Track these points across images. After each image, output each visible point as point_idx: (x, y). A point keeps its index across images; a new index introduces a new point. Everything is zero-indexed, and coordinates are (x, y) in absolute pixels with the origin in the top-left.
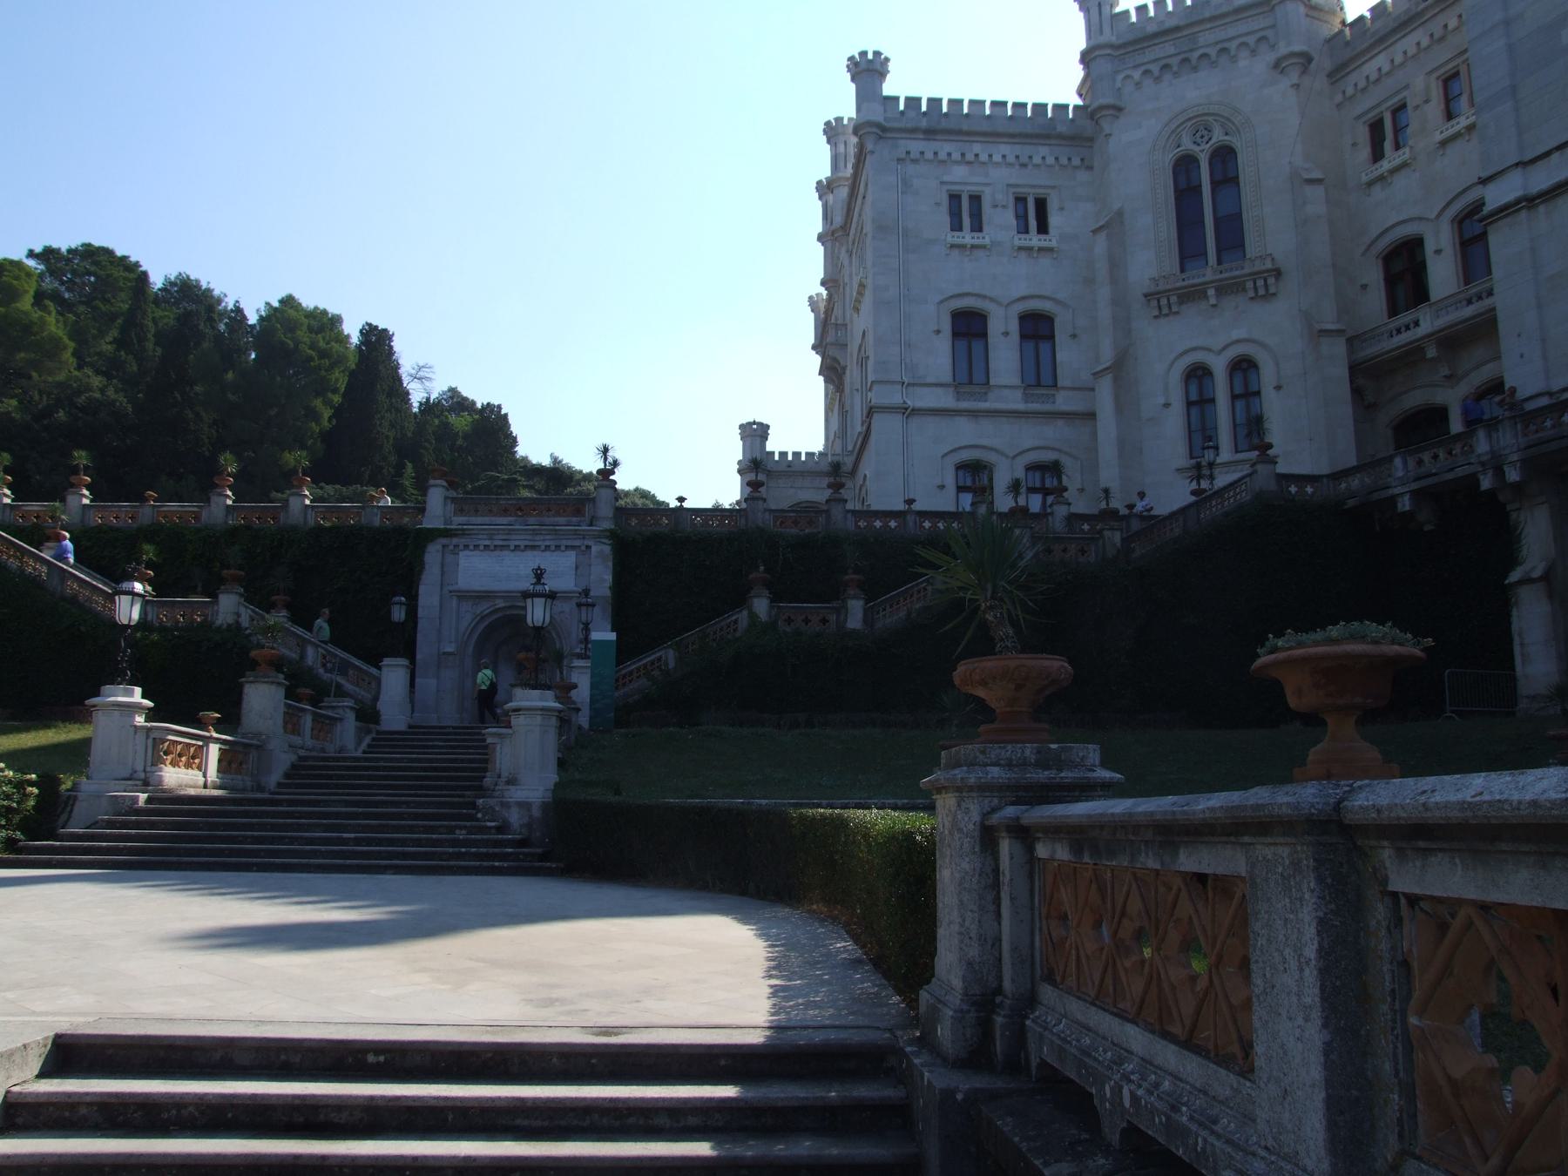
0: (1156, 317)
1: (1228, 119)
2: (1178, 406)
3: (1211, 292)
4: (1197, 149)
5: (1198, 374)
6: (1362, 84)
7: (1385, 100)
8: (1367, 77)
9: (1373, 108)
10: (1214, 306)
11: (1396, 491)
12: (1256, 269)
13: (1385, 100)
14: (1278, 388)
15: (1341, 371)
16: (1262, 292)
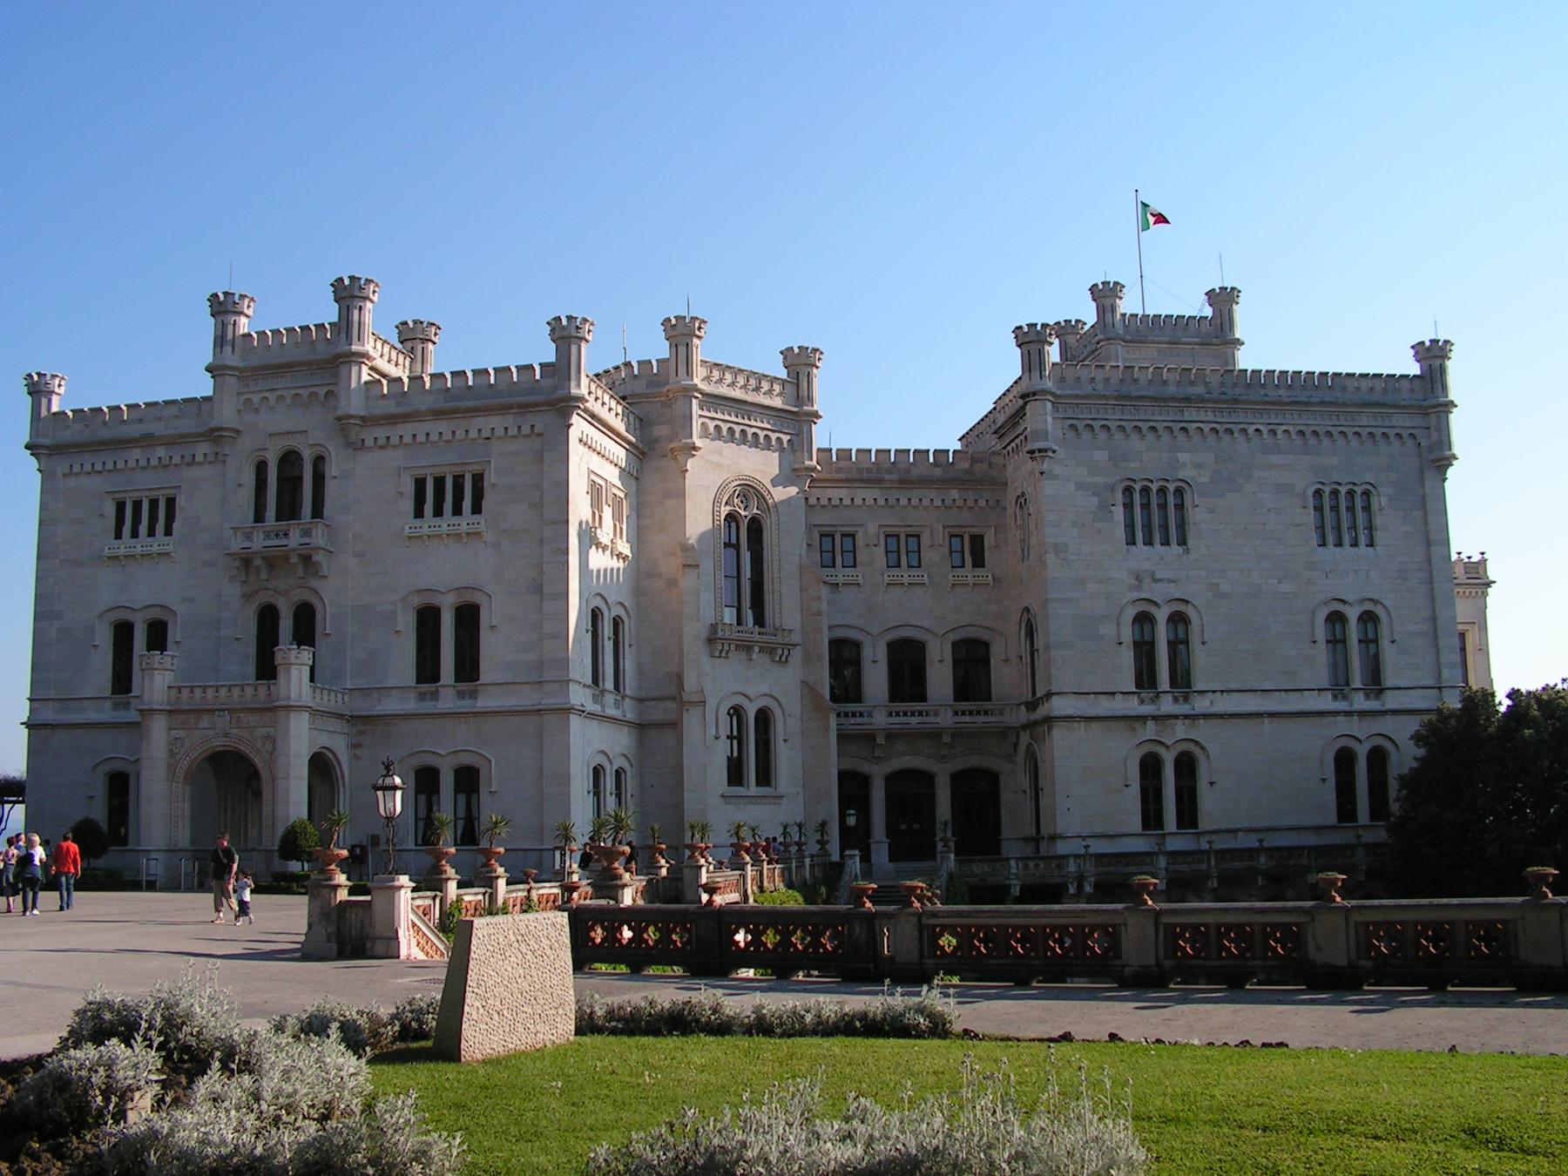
0: (713, 657)
1: (763, 497)
2: (723, 737)
3: (757, 649)
4: (743, 513)
5: (737, 712)
6: (824, 502)
7: (842, 526)
8: (830, 499)
9: (832, 526)
10: (751, 659)
11: (1012, 882)
12: (787, 640)
13: (842, 526)
14: (785, 741)
15: (833, 740)
16: (783, 659)
